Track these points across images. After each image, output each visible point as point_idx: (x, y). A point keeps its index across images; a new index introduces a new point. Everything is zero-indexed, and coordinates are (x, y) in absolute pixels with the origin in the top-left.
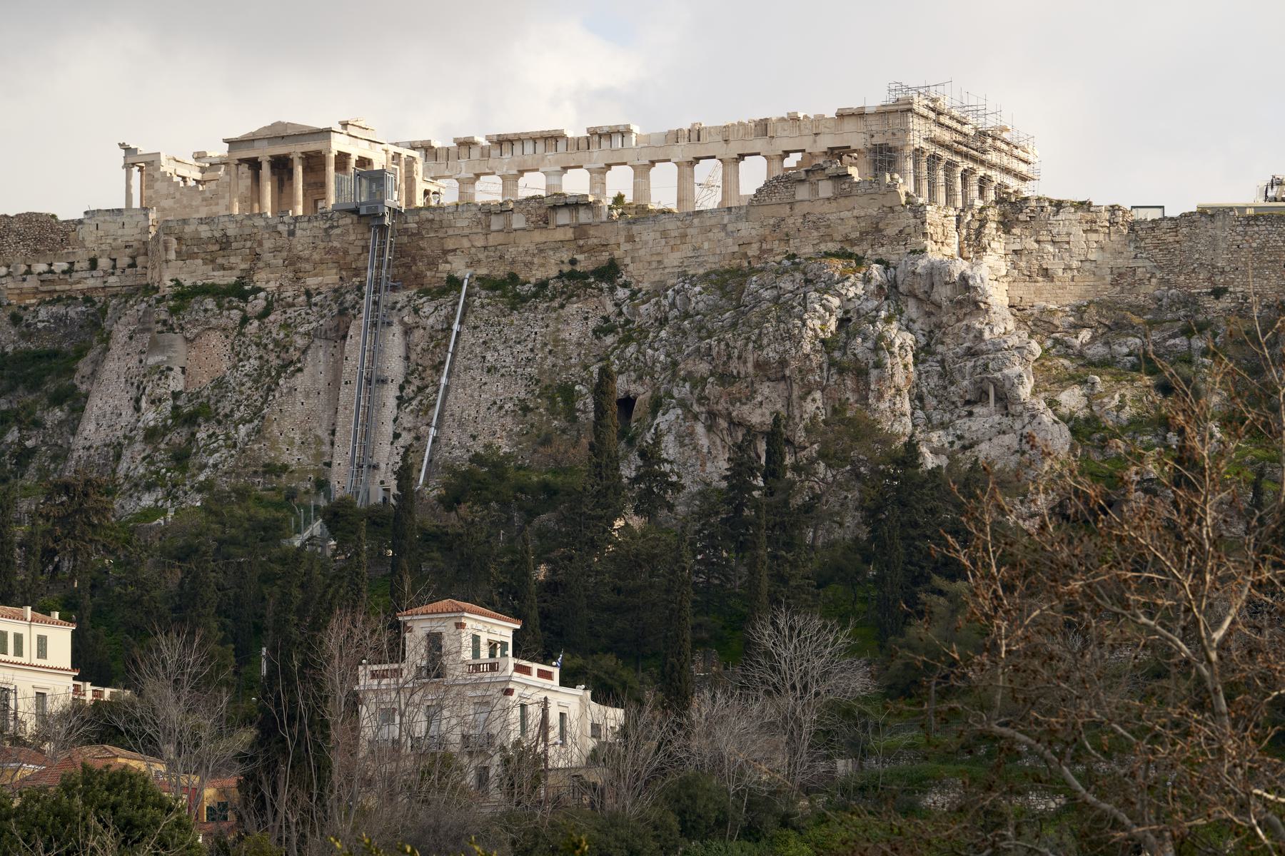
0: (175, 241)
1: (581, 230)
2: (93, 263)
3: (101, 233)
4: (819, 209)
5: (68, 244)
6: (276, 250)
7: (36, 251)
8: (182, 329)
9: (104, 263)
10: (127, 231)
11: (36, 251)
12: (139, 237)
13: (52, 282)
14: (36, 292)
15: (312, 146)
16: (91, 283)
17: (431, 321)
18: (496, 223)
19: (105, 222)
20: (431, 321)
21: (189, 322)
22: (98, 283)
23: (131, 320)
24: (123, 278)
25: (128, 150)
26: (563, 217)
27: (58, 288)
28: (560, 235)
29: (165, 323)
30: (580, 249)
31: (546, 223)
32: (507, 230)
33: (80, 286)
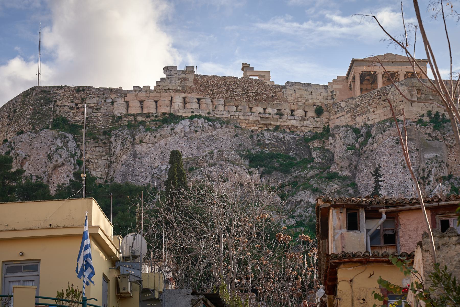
0: (416, 91)
3: (298, 95)
5: (277, 99)
7: (255, 100)
8: (445, 139)
9: (299, 113)
10: (314, 96)
11: (255, 100)
12: (322, 101)
13: (268, 119)
14: (258, 123)
16: (293, 123)
19: (300, 89)
21: (449, 136)
22: (298, 124)
23: (393, 133)
24: (314, 123)
27: (272, 123)
29: (429, 134)
33: (286, 124)
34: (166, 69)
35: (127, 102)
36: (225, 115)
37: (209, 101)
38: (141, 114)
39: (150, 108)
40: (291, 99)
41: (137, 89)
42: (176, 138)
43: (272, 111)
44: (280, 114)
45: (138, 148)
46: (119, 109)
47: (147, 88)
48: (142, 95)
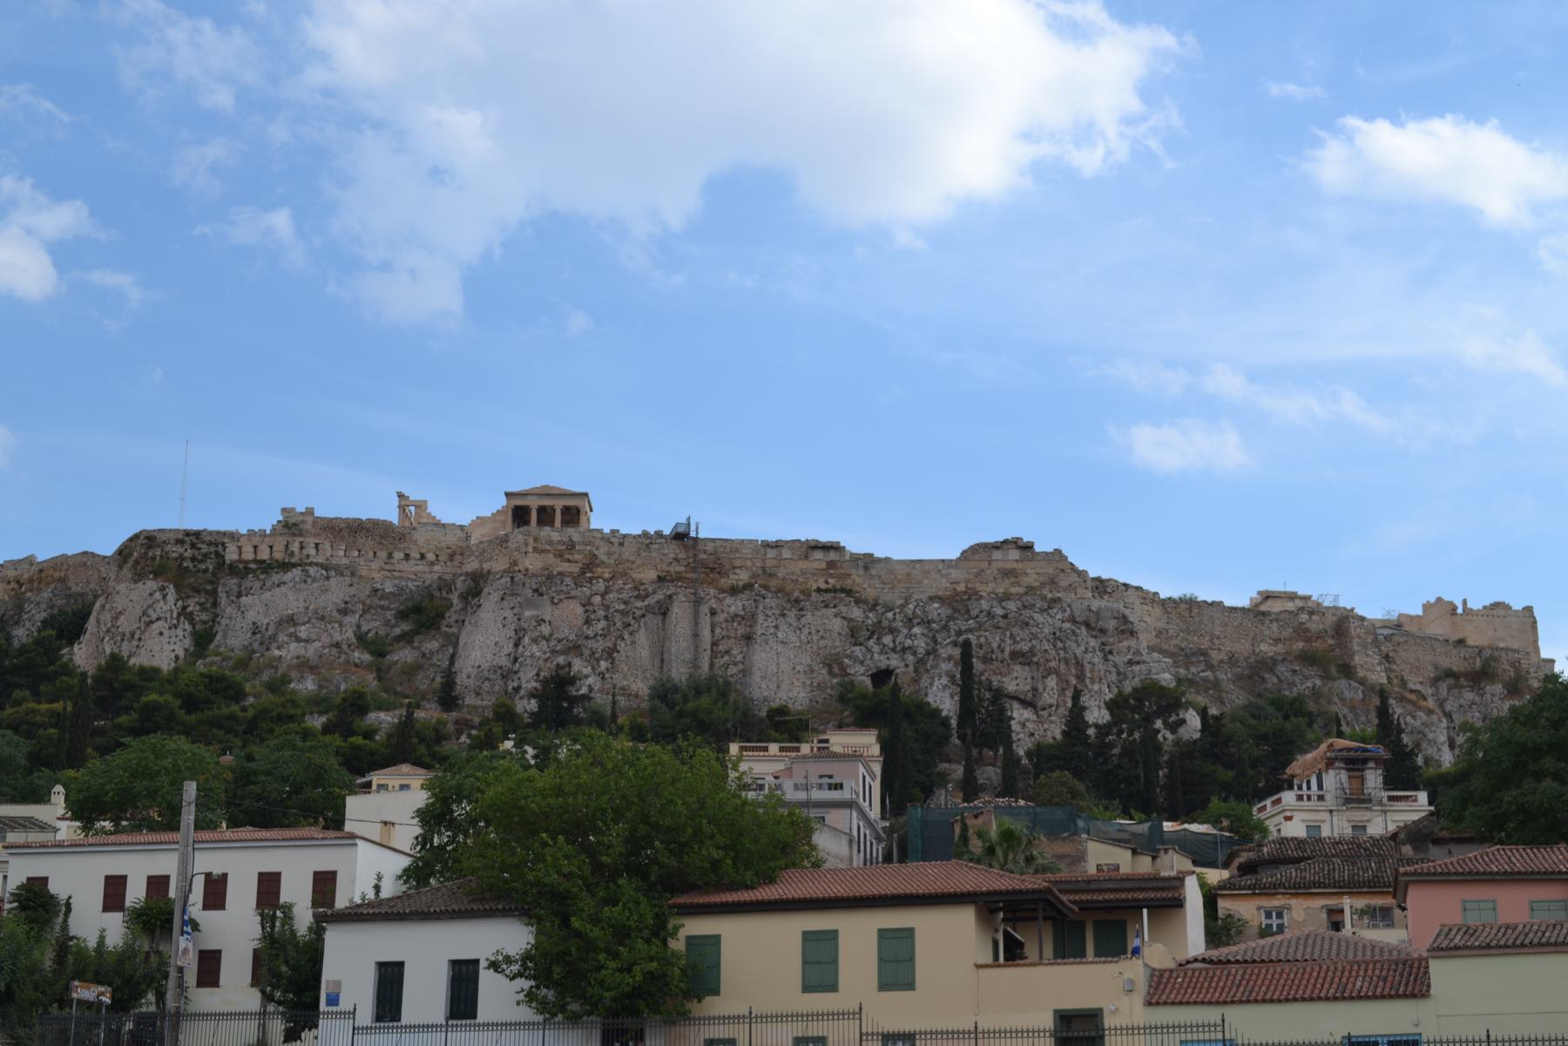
1: (831, 564)
2: (423, 557)
4: (1009, 566)
6: (609, 554)
9: (431, 557)
15: (571, 502)
16: (421, 568)
17: (732, 609)
18: (771, 553)
20: (732, 609)
25: (401, 496)
26: (818, 555)
28: (816, 565)
30: (831, 576)
31: (806, 557)
32: (780, 559)
34: (284, 510)
35: (240, 548)
36: (345, 561)
37: (328, 546)
38: (255, 561)
39: (264, 554)
40: (421, 542)
41: (251, 533)
42: (283, 588)
43: (398, 555)
44: (407, 557)
45: (244, 599)
46: (231, 555)
47: (263, 534)
48: (256, 540)
